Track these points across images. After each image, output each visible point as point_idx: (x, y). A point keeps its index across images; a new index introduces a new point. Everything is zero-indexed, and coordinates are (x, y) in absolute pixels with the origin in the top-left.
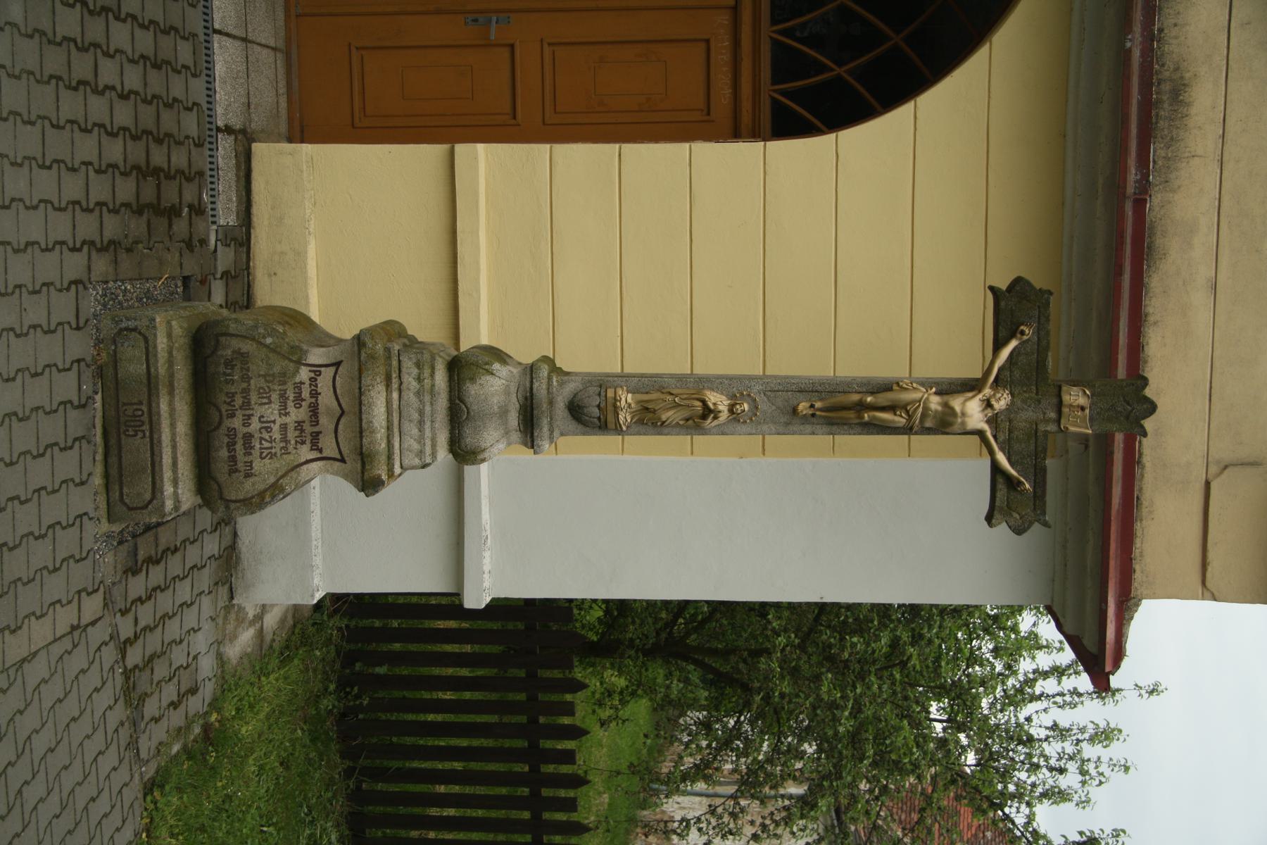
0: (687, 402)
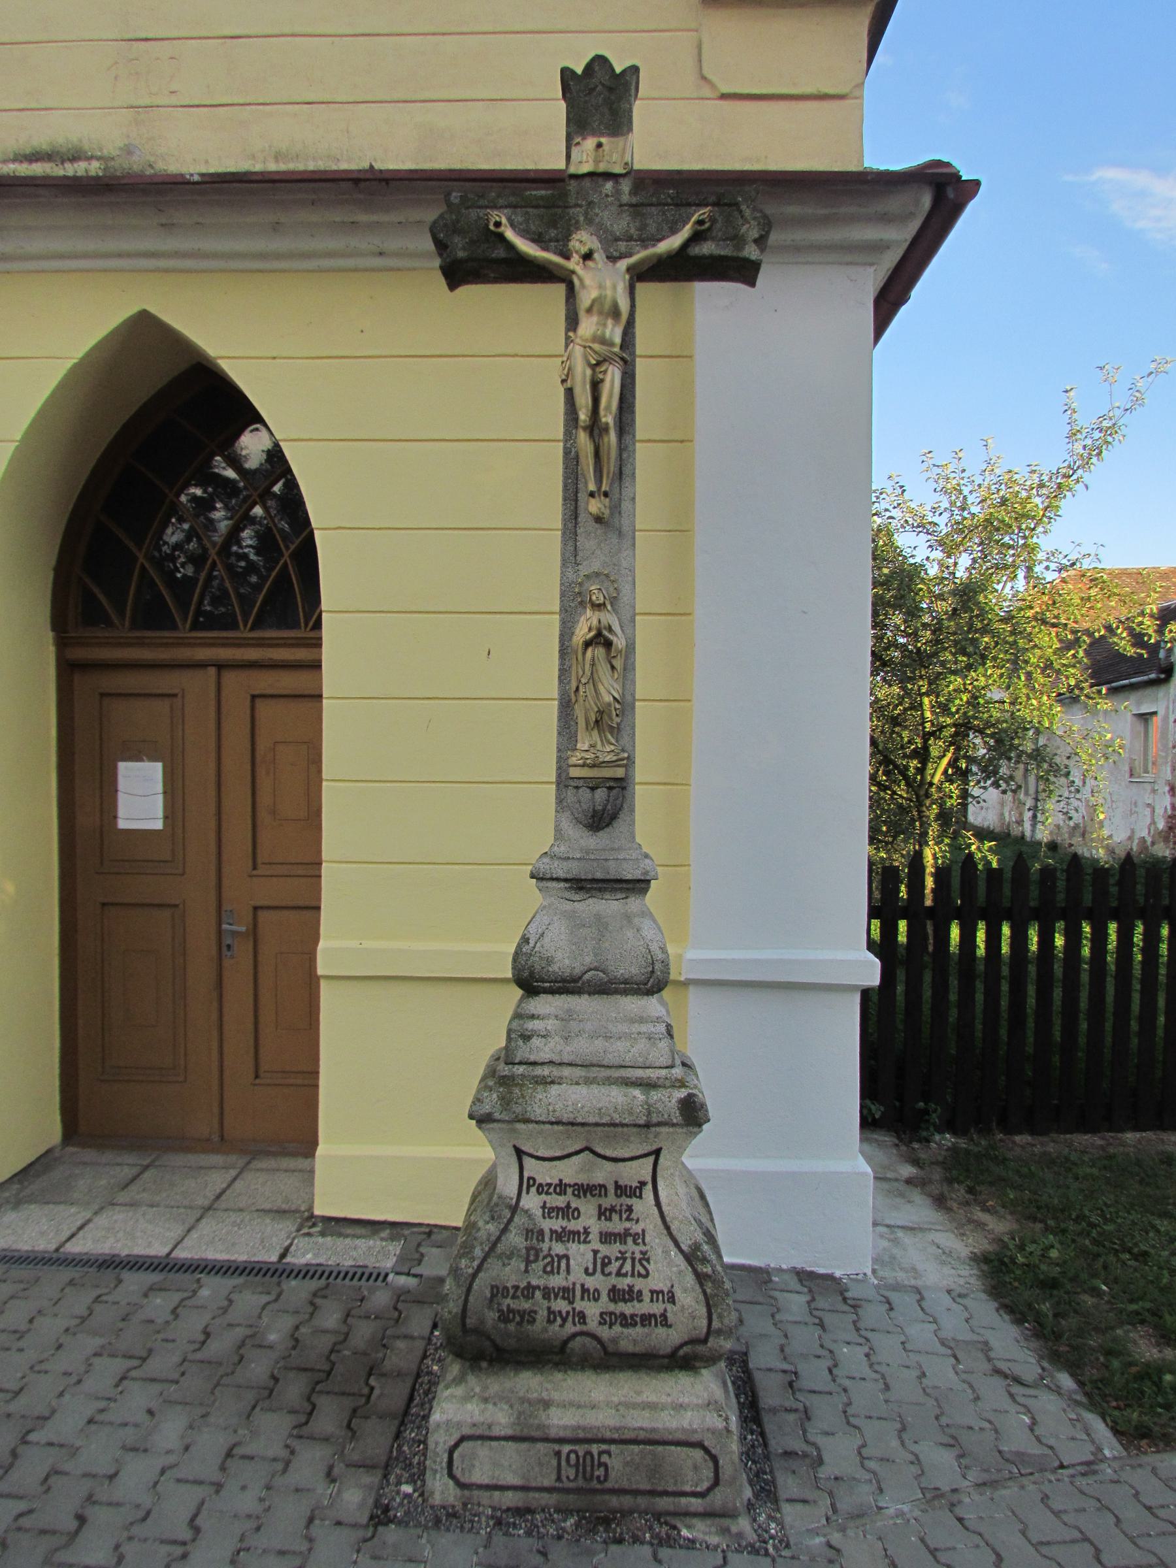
0: (587, 666)
